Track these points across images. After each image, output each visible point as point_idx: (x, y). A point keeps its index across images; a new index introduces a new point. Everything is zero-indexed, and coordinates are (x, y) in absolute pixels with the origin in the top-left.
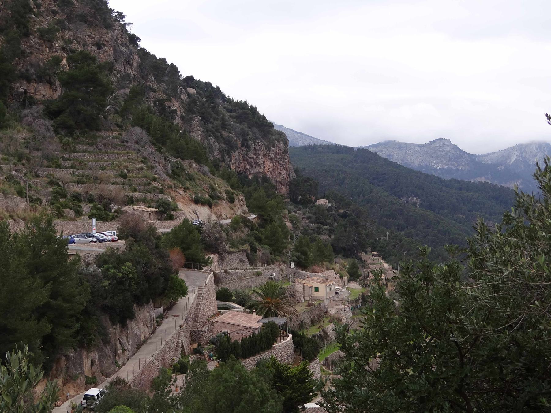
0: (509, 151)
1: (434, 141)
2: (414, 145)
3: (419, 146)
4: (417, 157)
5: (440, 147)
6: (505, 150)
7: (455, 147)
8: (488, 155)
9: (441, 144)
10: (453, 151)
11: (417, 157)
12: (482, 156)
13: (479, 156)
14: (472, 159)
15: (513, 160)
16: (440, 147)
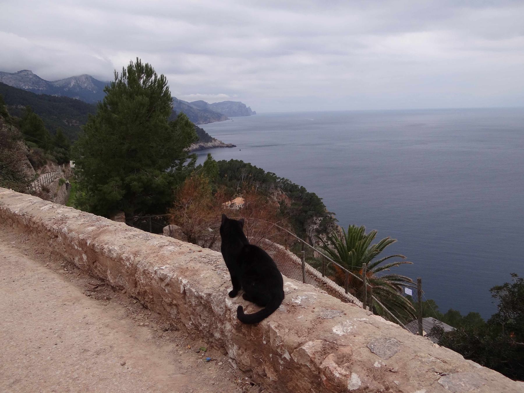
0: (70, 79)
1: (21, 72)
2: (6, 73)
3: (10, 74)
4: (10, 81)
5: (25, 75)
6: (67, 79)
7: (36, 76)
8: (57, 81)
9: (26, 74)
10: (34, 78)
11: (10, 81)
12: (52, 82)
13: (51, 82)
14: (48, 84)
15: (72, 85)
16: (24, 74)
